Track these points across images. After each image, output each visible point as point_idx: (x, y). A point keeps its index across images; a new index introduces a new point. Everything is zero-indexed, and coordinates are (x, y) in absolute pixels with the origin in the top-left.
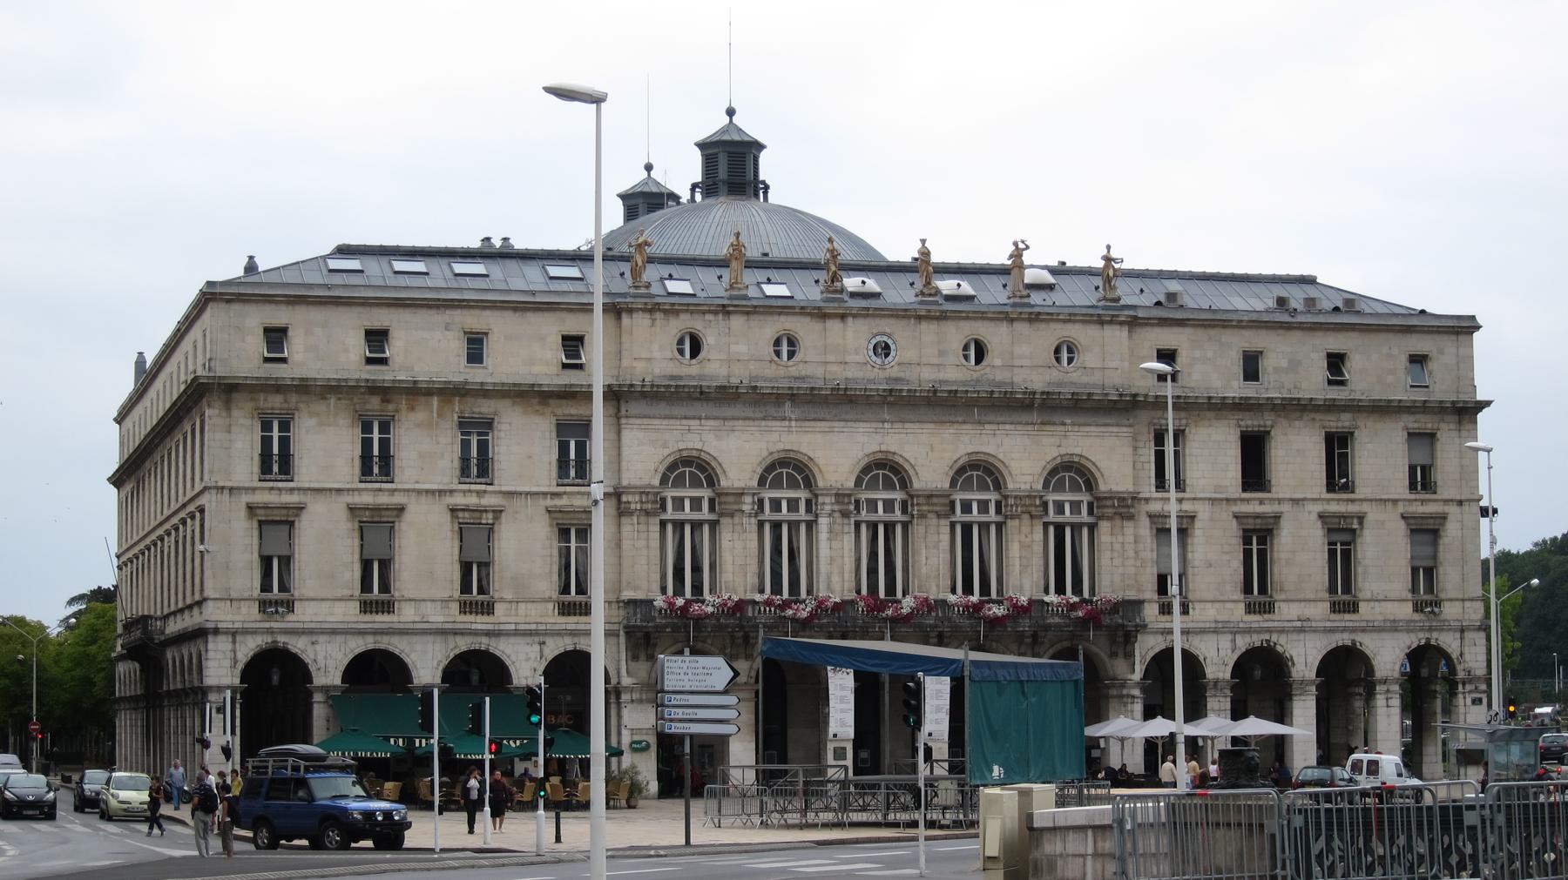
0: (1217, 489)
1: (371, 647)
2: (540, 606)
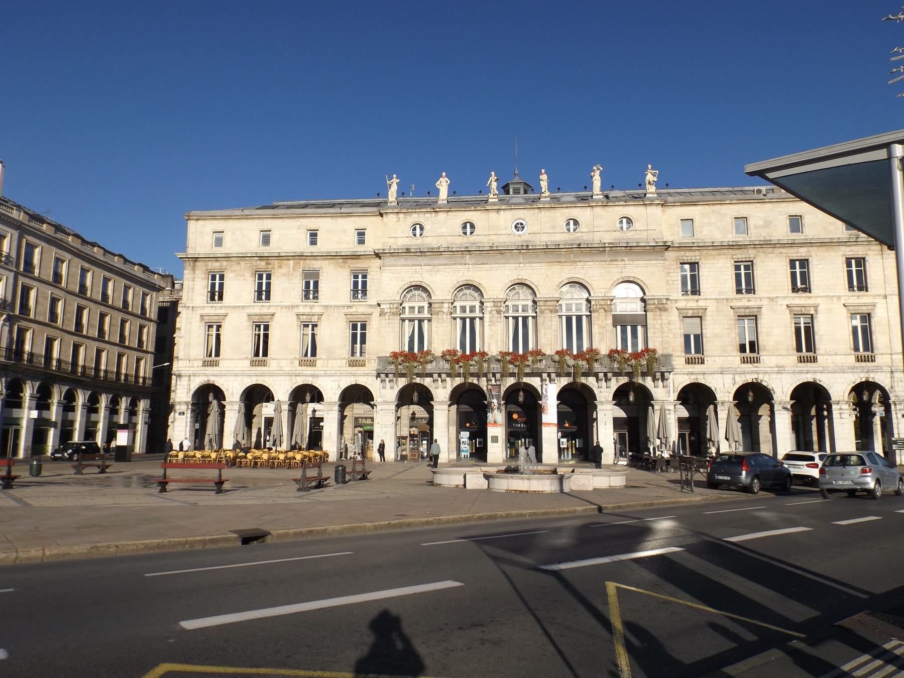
0: (720, 293)
2: (339, 361)
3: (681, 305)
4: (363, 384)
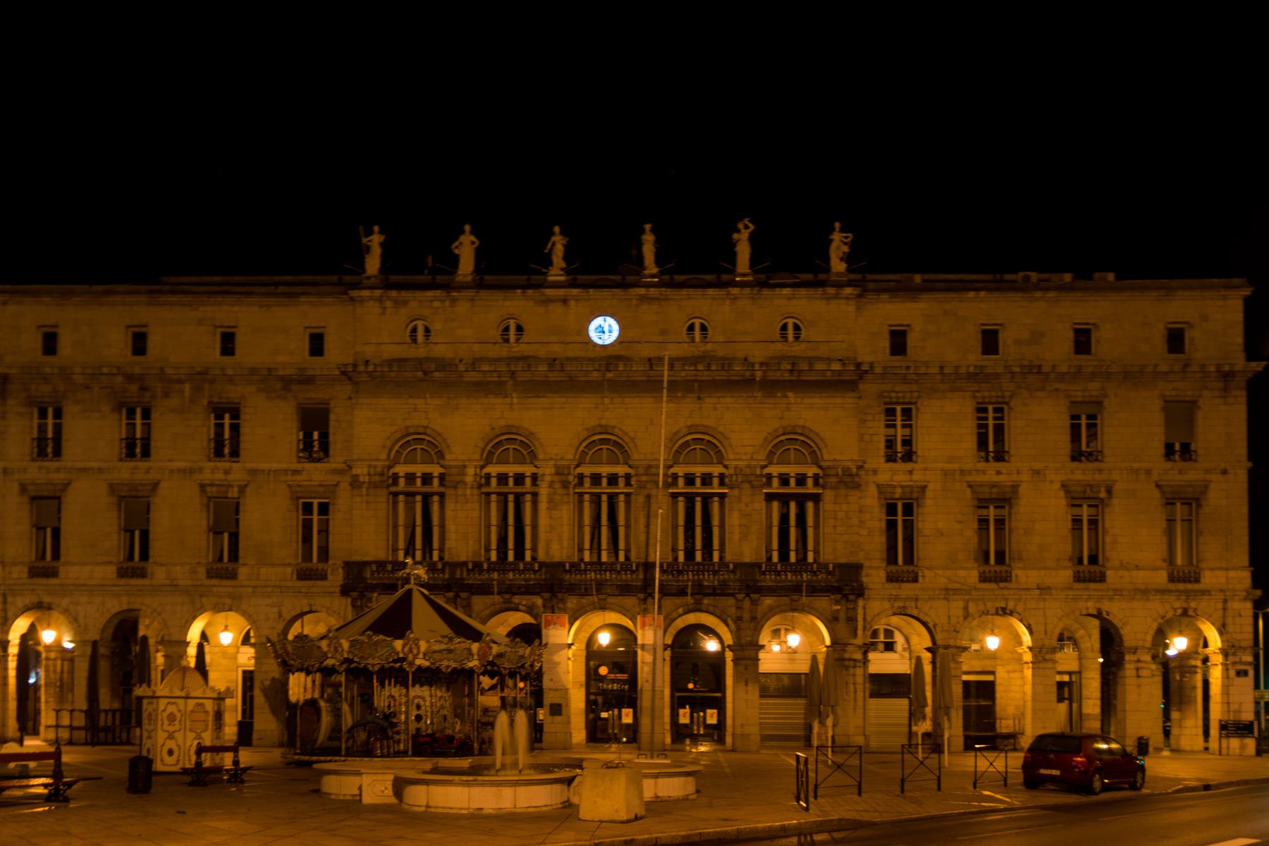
1: (125, 607)
3: (883, 478)
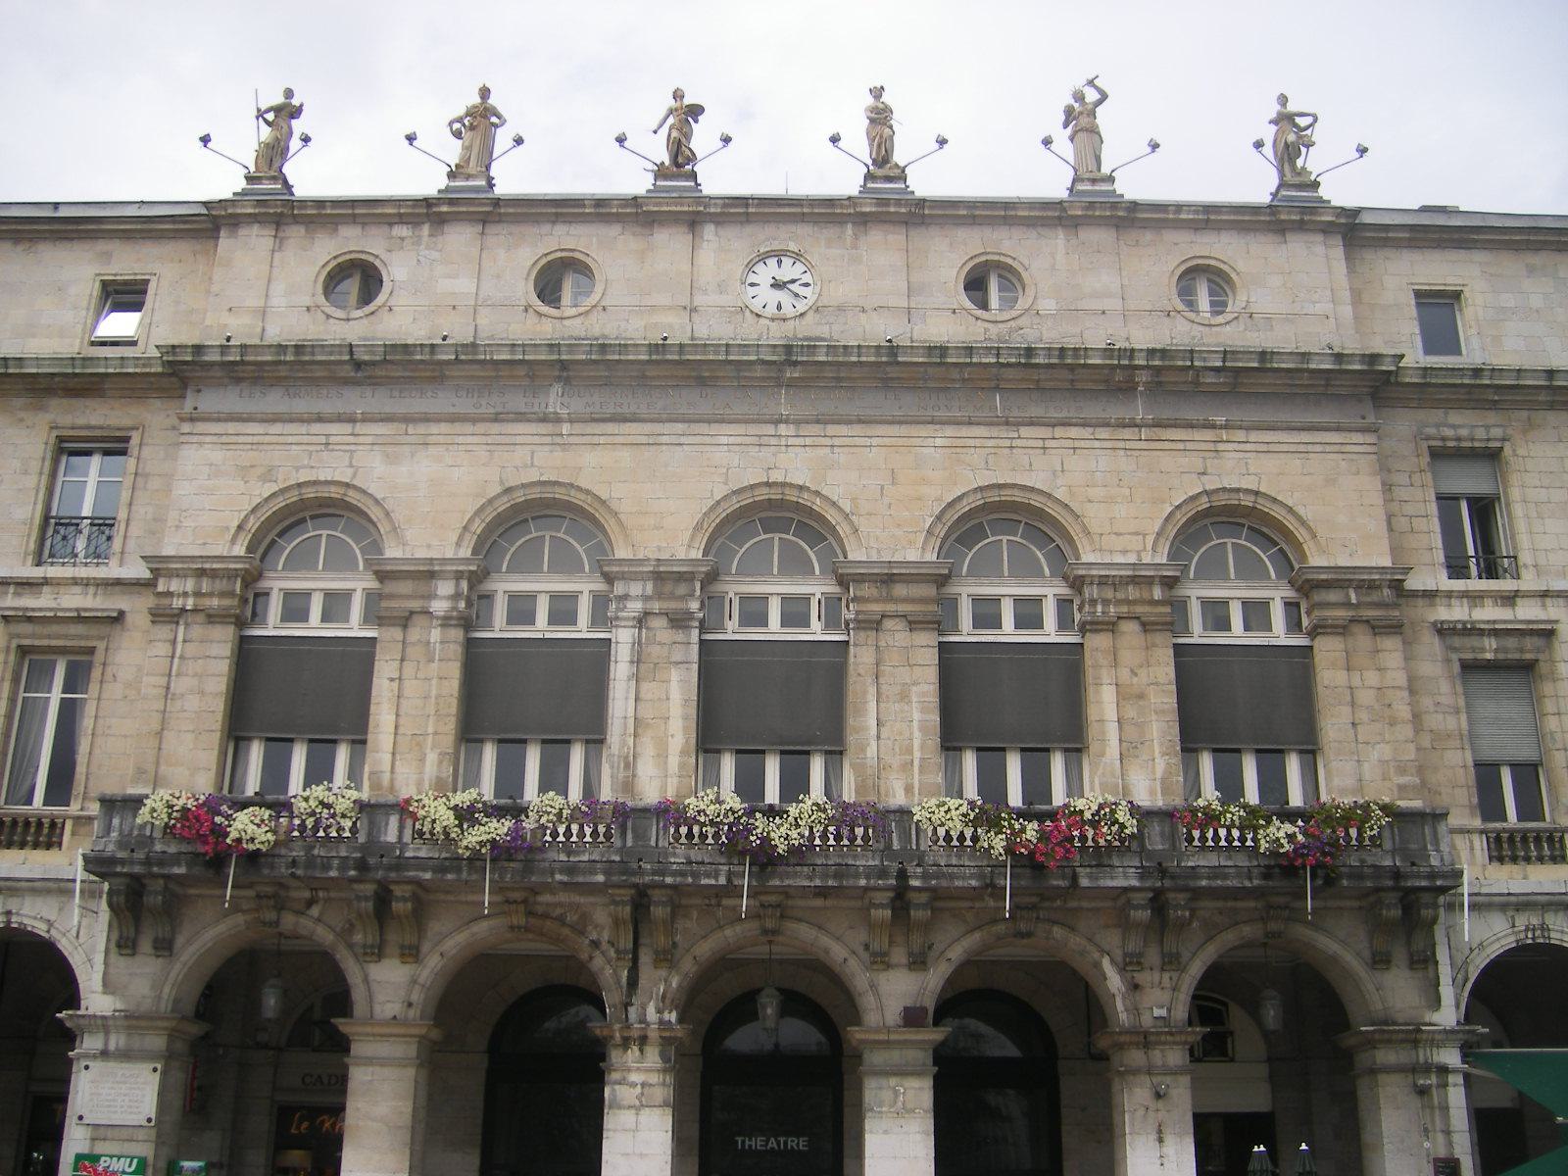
4: (41, 929)
